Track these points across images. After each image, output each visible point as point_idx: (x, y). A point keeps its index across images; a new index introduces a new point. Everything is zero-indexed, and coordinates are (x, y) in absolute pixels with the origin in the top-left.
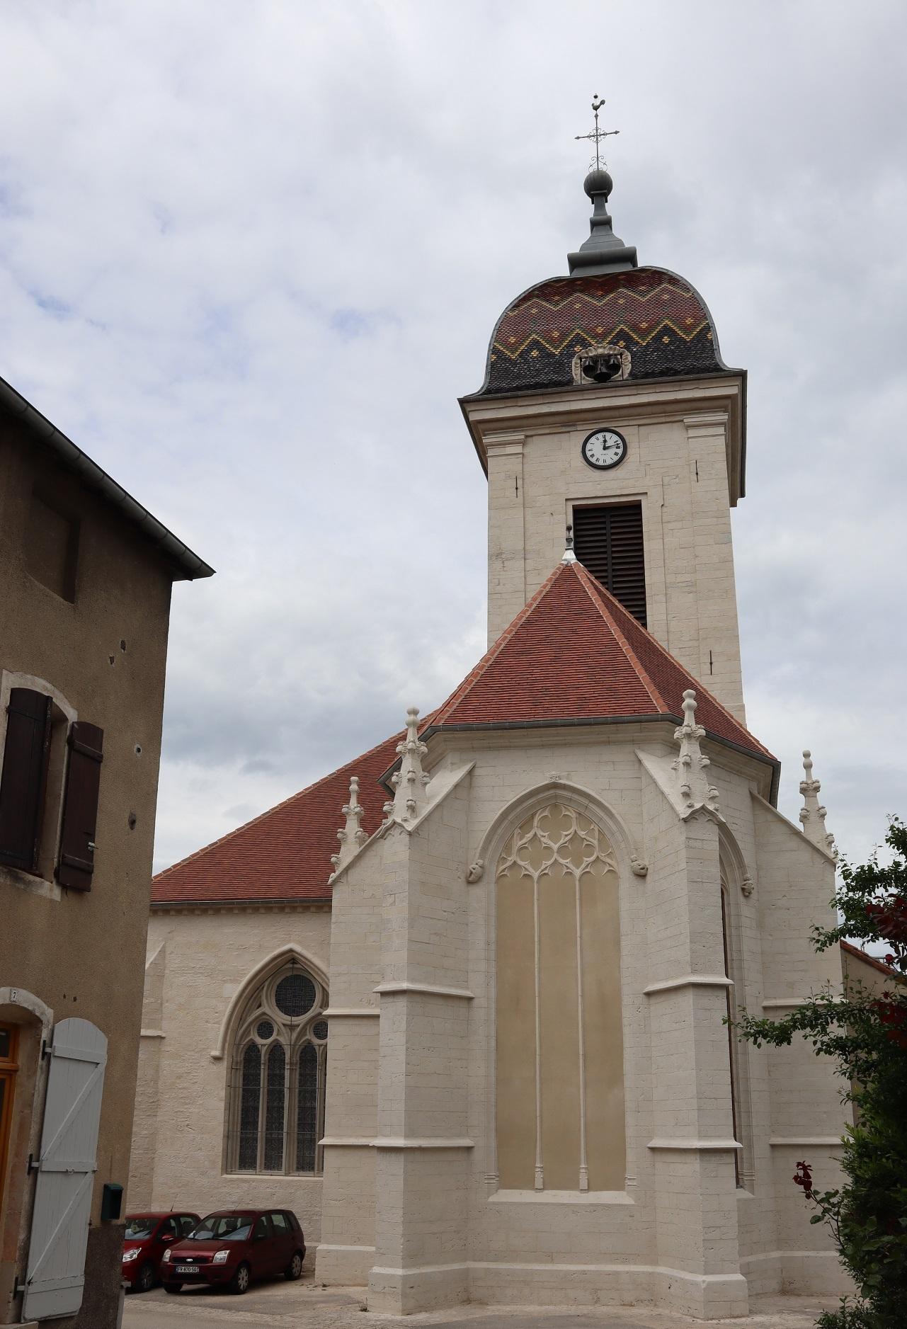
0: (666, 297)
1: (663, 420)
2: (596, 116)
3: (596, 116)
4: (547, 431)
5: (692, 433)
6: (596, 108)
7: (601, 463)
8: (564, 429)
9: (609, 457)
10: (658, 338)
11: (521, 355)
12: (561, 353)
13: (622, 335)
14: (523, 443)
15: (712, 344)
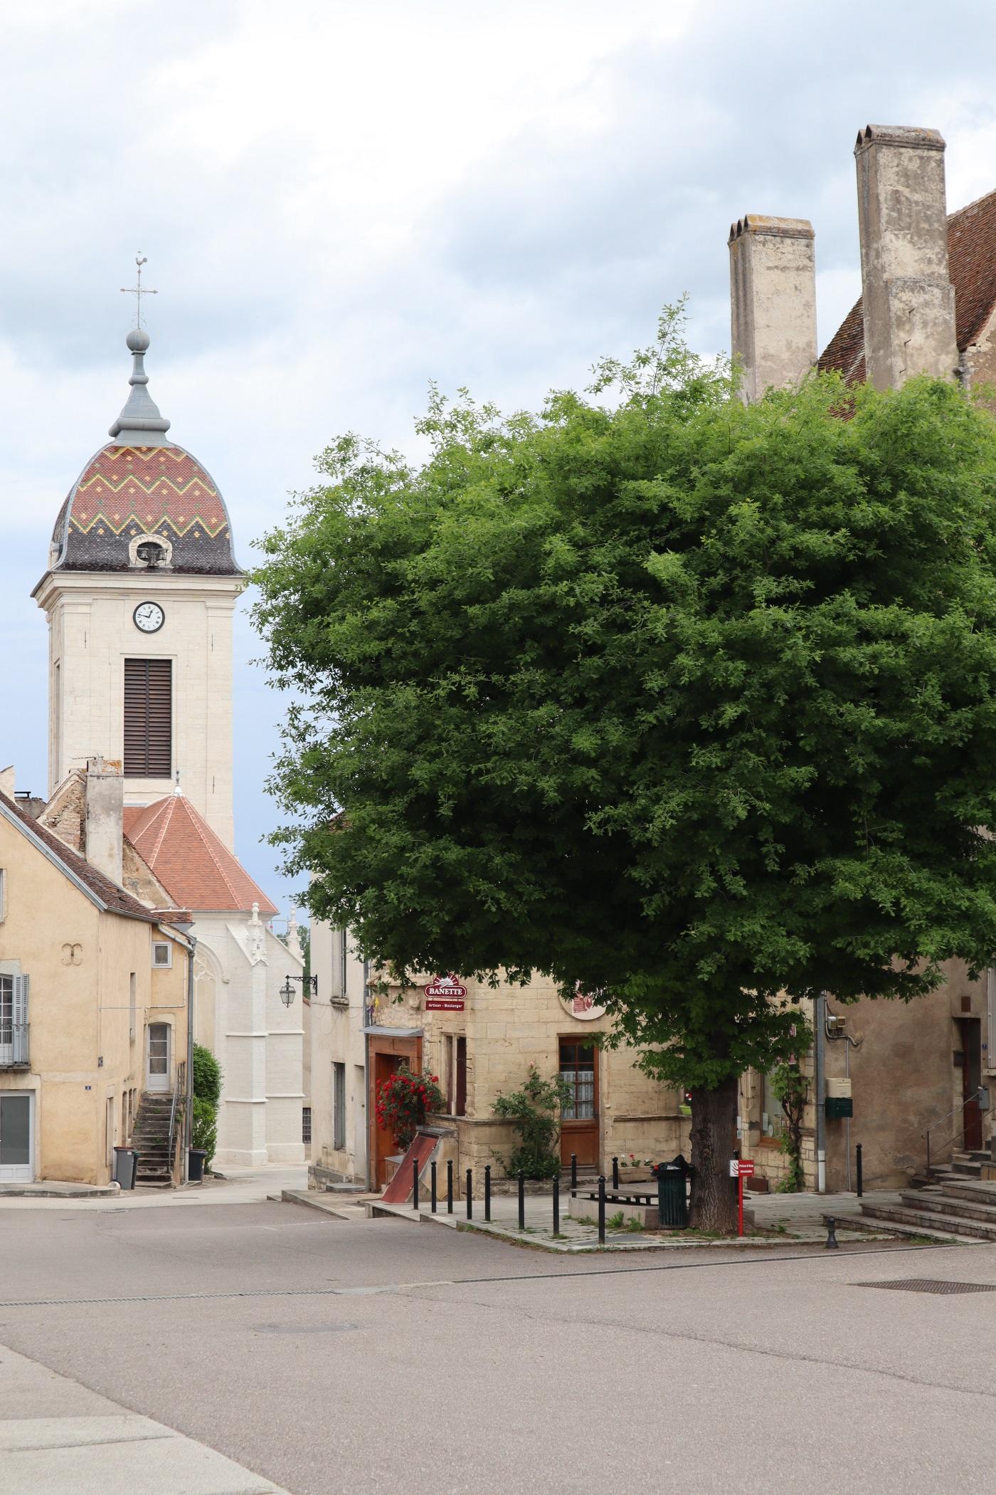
0: (197, 493)
1: (191, 599)
2: (139, 272)
3: (139, 272)
4: (109, 597)
5: (211, 612)
6: (139, 264)
7: (146, 628)
8: (120, 597)
9: (150, 624)
10: (191, 532)
11: (90, 532)
12: (120, 535)
13: (166, 526)
14: (90, 604)
15: (229, 543)
